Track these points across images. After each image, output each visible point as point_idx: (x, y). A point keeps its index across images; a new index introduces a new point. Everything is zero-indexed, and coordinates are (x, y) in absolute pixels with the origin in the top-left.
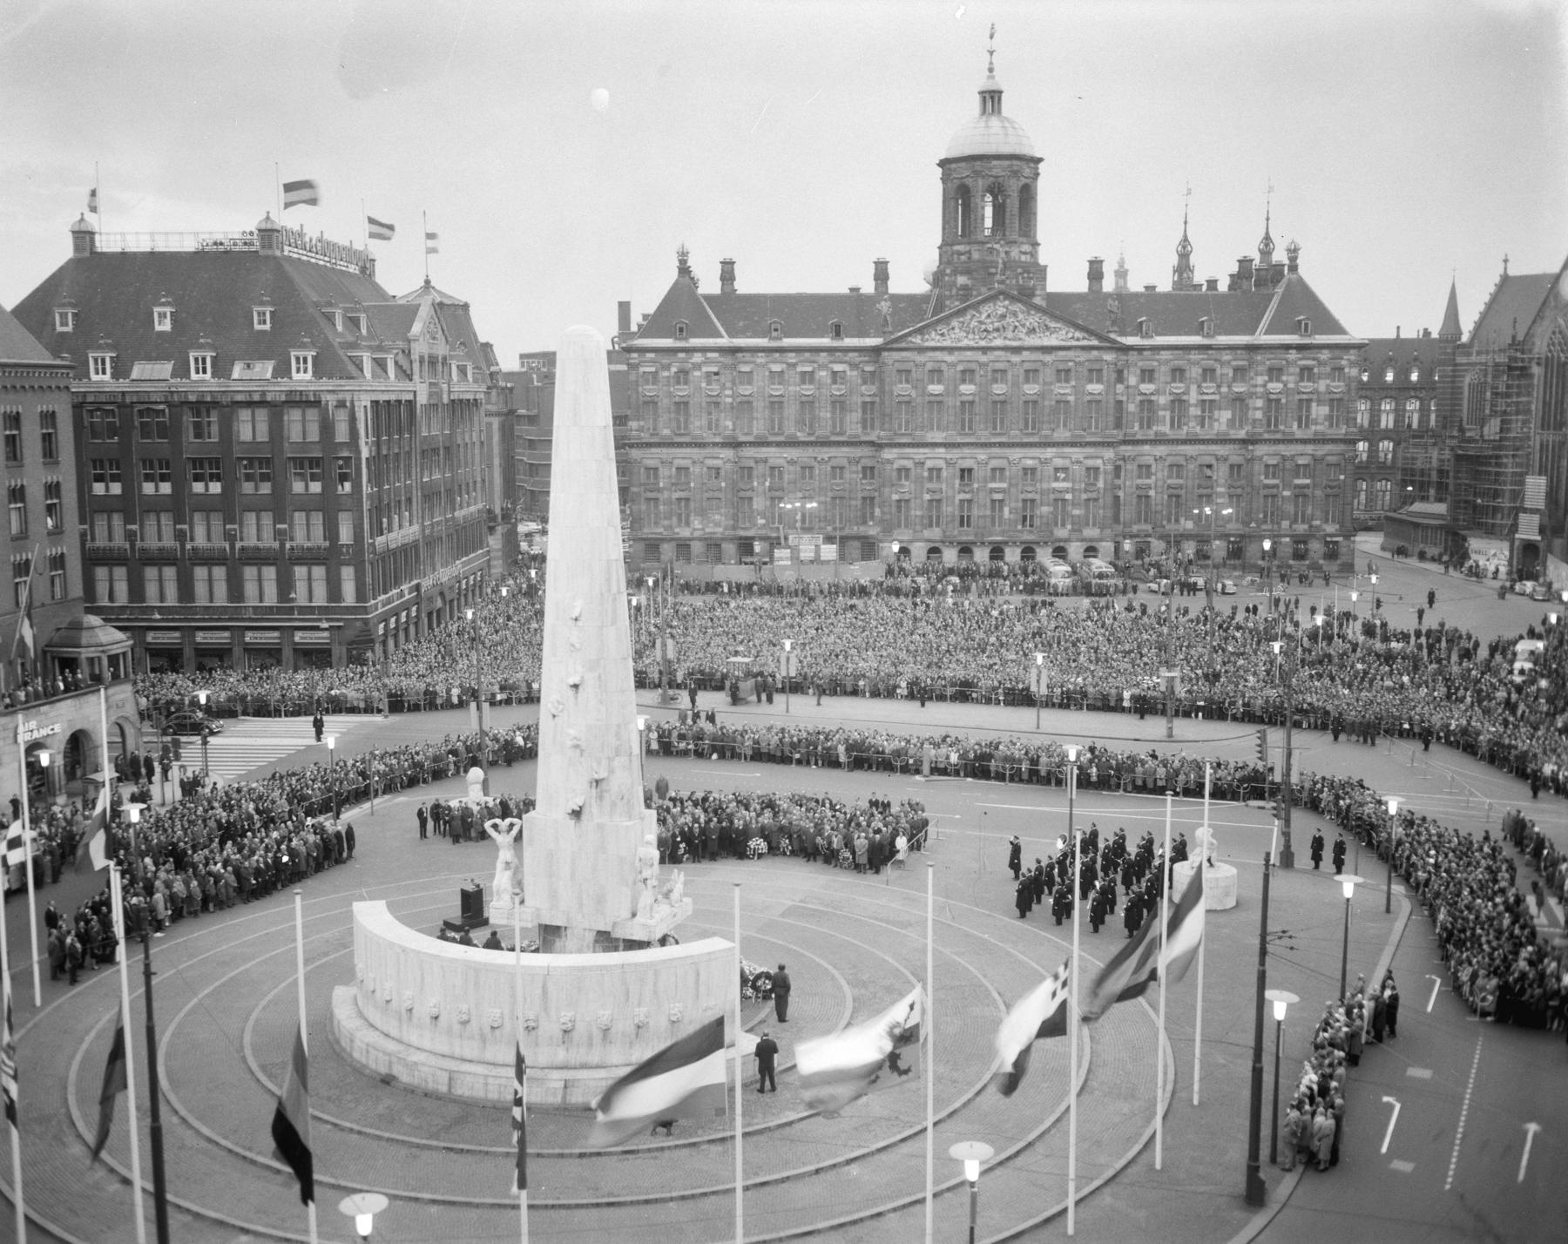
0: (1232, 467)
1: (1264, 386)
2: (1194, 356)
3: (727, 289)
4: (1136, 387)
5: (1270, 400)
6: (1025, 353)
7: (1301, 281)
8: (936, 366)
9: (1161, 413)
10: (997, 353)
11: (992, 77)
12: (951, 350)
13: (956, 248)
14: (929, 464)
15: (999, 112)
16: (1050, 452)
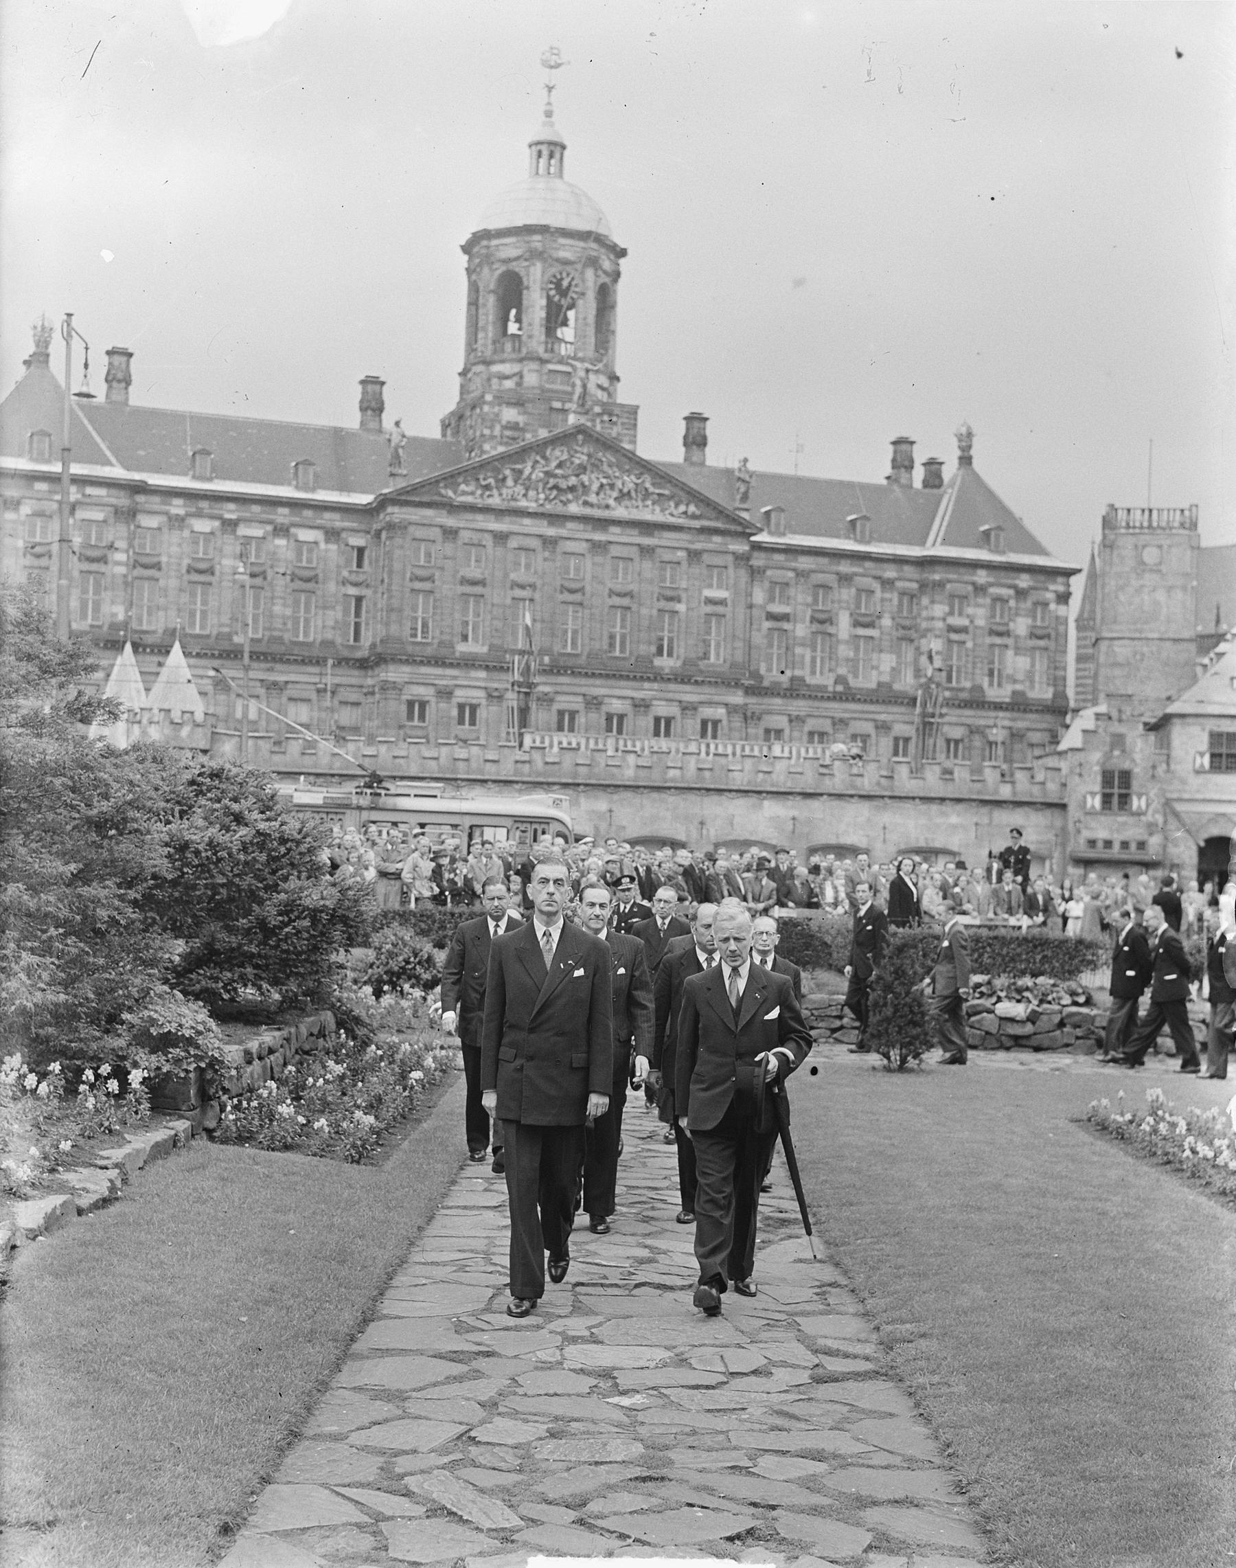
0: (896, 739)
1: (944, 620)
2: (845, 567)
3: (117, 397)
4: (763, 607)
5: (950, 641)
6: (615, 529)
7: (977, 477)
8: (476, 537)
9: (798, 650)
10: (570, 525)
11: (552, 125)
12: (499, 513)
13: (496, 368)
14: (460, 695)
15: (560, 174)
16: (647, 691)
